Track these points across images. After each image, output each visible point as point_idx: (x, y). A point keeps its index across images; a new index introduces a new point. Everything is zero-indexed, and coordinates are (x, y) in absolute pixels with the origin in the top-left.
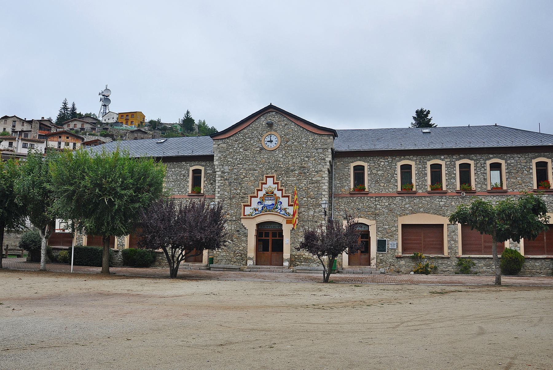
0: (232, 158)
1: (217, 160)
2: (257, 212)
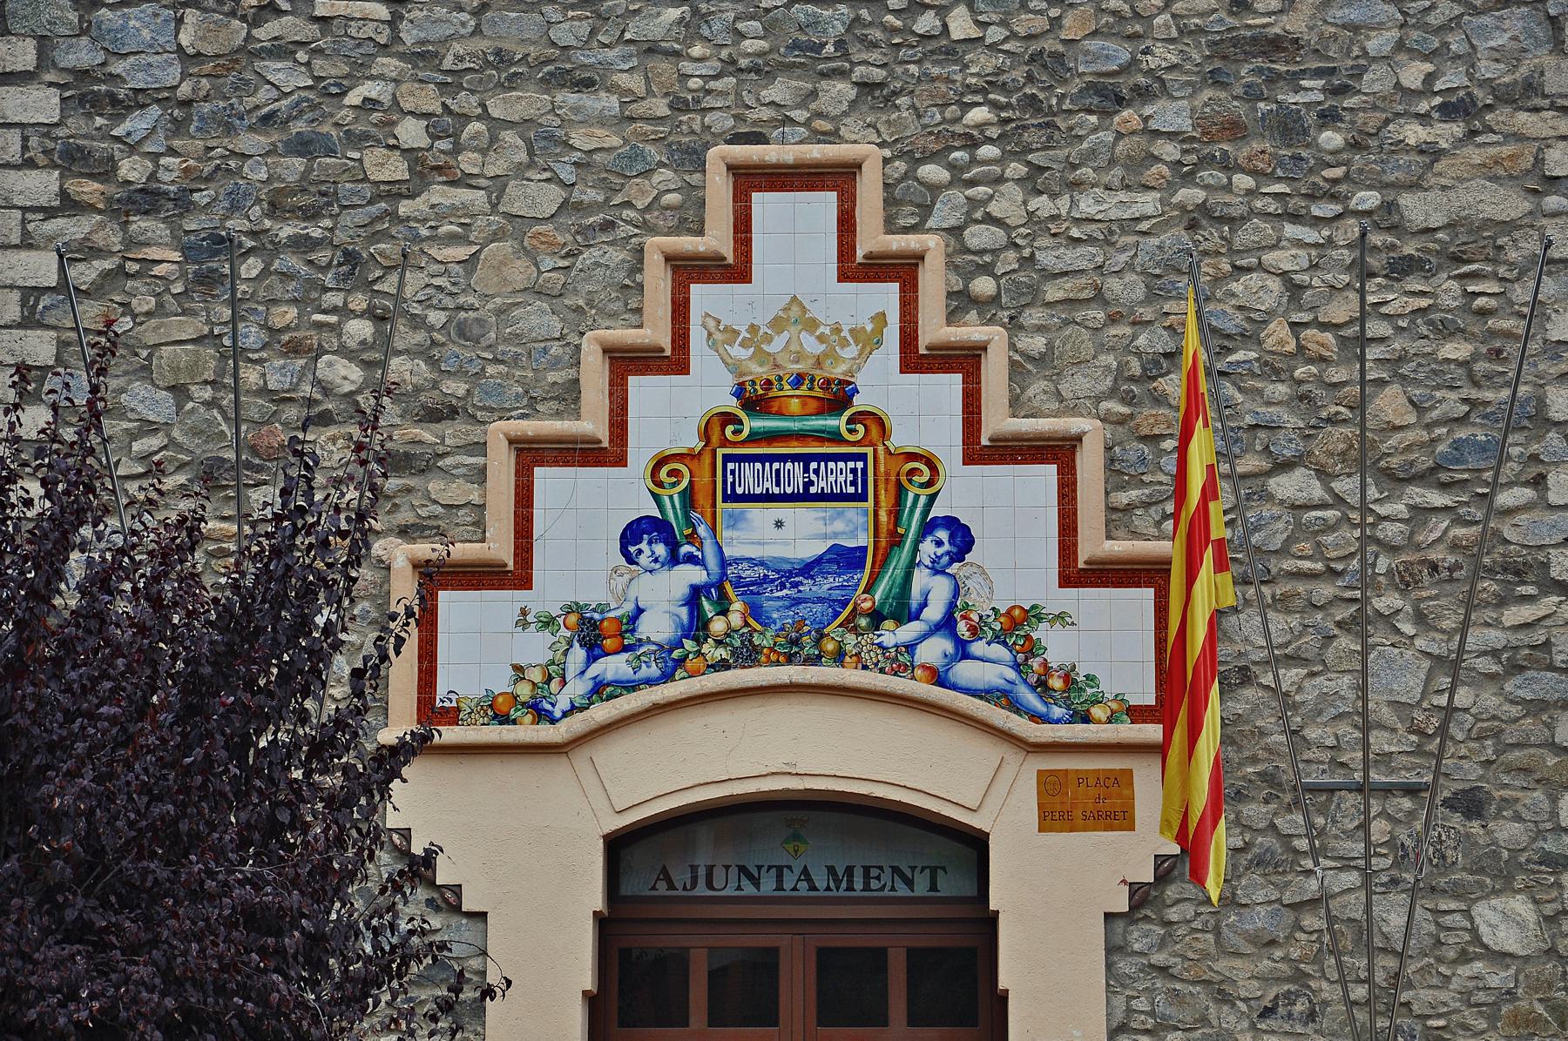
2: (614, 666)
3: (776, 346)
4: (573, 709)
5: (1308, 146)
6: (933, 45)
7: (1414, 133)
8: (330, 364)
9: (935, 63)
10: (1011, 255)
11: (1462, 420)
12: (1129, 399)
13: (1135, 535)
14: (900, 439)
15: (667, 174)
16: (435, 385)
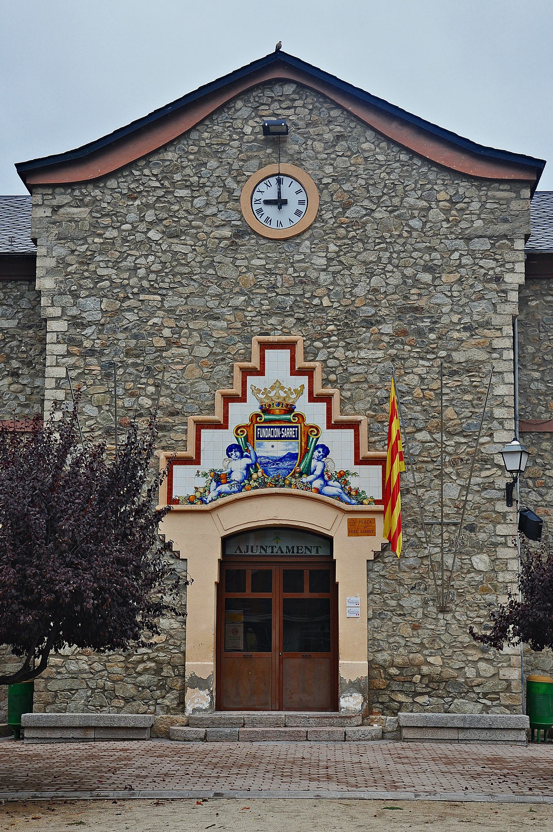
0: (116, 265)
1: (50, 272)
2: (225, 488)
3: (272, 395)
5: (426, 338)
6: (318, 307)
7: (456, 335)
8: (142, 399)
9: (318, 313)
10: (341, 368)
11: (470, 417)
13: (377, 450)
14: (309, 421)
15: (241, 344)
16: (173, 405)
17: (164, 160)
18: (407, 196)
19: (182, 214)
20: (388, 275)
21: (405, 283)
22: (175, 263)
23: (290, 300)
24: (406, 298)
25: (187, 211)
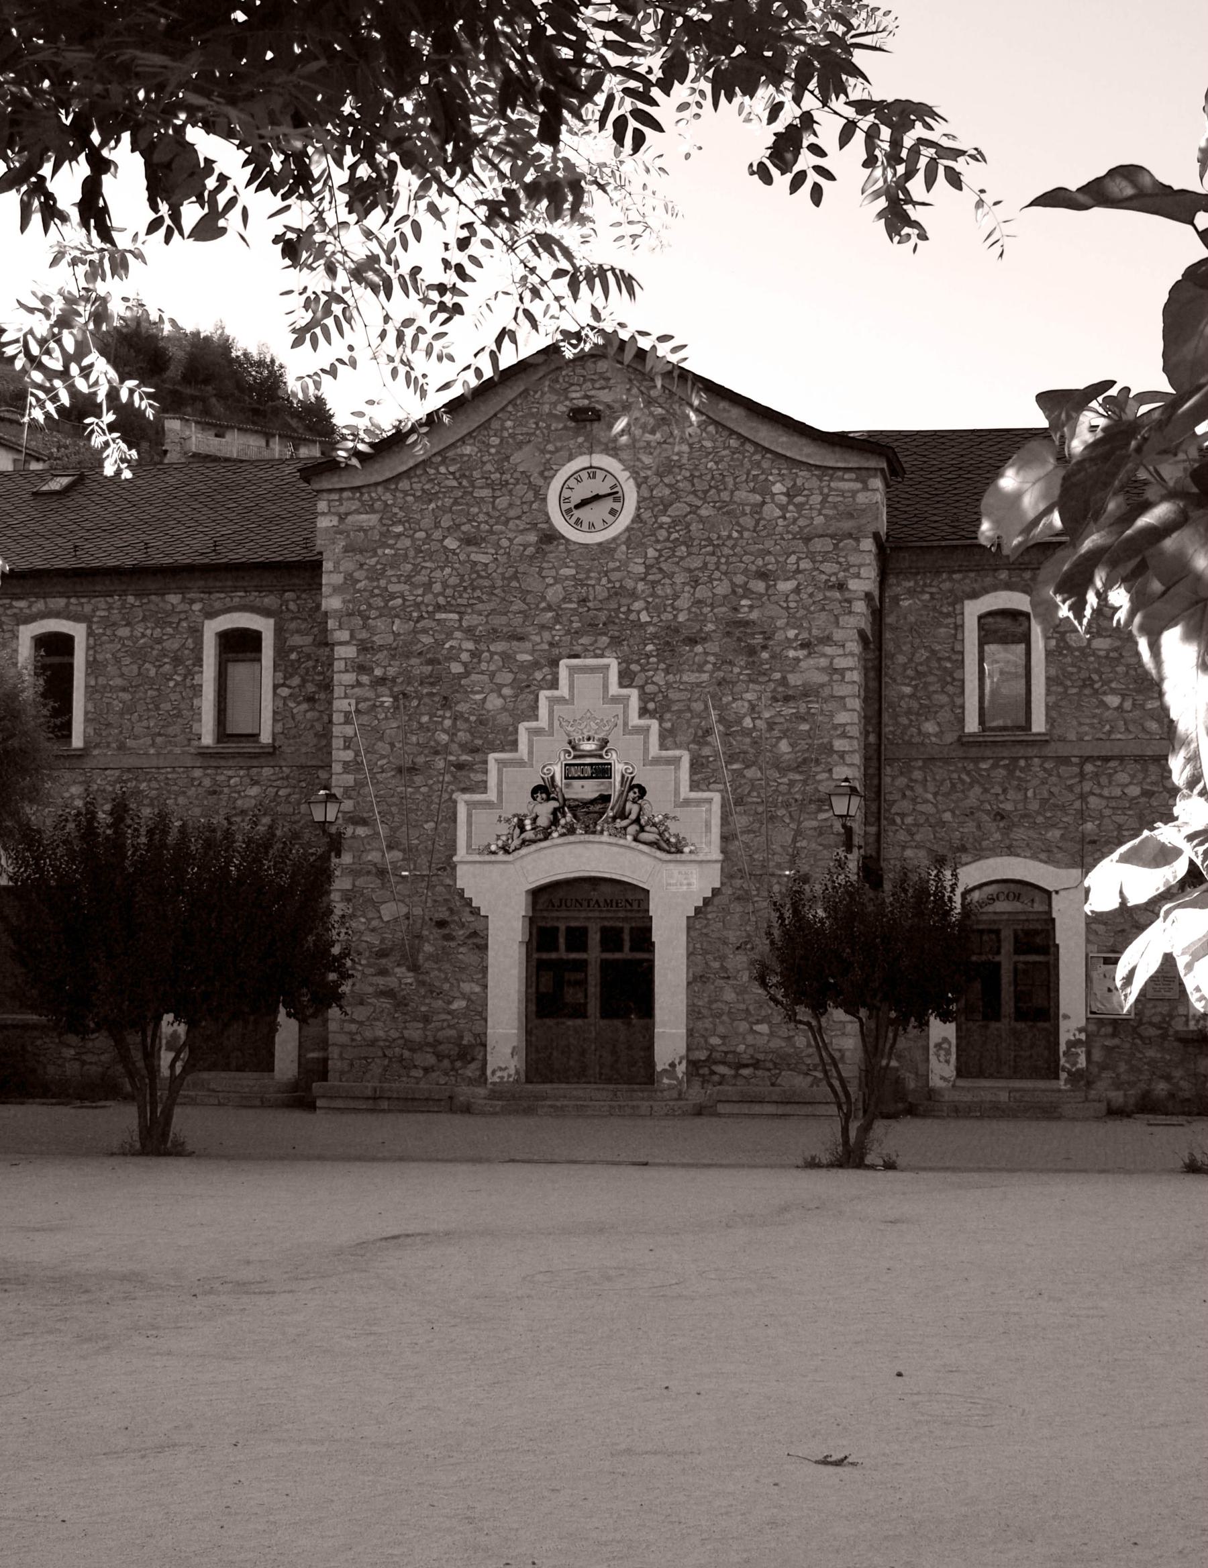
0: (408, 579)
1: (336, 590)
4: (516, 849)
7: (792, 654)
12: (698, 743)
17: (462, 455)
18: (737, 489)
19: (482, 517)
20: (715, 583)
21: (734, 592)
22: (474, 576)
23: (603, 616)
24: (736, 610)
25: (487, 514)
